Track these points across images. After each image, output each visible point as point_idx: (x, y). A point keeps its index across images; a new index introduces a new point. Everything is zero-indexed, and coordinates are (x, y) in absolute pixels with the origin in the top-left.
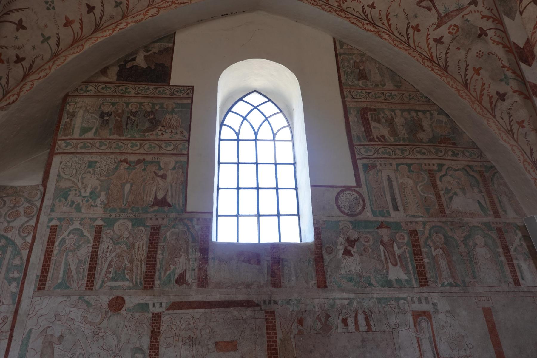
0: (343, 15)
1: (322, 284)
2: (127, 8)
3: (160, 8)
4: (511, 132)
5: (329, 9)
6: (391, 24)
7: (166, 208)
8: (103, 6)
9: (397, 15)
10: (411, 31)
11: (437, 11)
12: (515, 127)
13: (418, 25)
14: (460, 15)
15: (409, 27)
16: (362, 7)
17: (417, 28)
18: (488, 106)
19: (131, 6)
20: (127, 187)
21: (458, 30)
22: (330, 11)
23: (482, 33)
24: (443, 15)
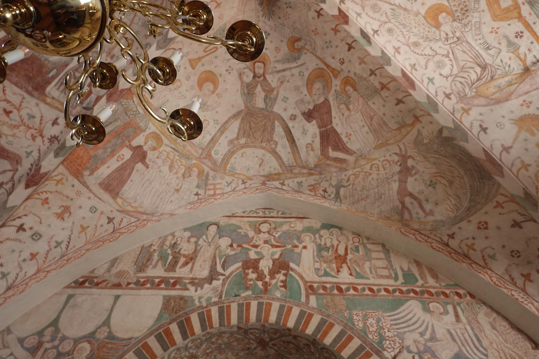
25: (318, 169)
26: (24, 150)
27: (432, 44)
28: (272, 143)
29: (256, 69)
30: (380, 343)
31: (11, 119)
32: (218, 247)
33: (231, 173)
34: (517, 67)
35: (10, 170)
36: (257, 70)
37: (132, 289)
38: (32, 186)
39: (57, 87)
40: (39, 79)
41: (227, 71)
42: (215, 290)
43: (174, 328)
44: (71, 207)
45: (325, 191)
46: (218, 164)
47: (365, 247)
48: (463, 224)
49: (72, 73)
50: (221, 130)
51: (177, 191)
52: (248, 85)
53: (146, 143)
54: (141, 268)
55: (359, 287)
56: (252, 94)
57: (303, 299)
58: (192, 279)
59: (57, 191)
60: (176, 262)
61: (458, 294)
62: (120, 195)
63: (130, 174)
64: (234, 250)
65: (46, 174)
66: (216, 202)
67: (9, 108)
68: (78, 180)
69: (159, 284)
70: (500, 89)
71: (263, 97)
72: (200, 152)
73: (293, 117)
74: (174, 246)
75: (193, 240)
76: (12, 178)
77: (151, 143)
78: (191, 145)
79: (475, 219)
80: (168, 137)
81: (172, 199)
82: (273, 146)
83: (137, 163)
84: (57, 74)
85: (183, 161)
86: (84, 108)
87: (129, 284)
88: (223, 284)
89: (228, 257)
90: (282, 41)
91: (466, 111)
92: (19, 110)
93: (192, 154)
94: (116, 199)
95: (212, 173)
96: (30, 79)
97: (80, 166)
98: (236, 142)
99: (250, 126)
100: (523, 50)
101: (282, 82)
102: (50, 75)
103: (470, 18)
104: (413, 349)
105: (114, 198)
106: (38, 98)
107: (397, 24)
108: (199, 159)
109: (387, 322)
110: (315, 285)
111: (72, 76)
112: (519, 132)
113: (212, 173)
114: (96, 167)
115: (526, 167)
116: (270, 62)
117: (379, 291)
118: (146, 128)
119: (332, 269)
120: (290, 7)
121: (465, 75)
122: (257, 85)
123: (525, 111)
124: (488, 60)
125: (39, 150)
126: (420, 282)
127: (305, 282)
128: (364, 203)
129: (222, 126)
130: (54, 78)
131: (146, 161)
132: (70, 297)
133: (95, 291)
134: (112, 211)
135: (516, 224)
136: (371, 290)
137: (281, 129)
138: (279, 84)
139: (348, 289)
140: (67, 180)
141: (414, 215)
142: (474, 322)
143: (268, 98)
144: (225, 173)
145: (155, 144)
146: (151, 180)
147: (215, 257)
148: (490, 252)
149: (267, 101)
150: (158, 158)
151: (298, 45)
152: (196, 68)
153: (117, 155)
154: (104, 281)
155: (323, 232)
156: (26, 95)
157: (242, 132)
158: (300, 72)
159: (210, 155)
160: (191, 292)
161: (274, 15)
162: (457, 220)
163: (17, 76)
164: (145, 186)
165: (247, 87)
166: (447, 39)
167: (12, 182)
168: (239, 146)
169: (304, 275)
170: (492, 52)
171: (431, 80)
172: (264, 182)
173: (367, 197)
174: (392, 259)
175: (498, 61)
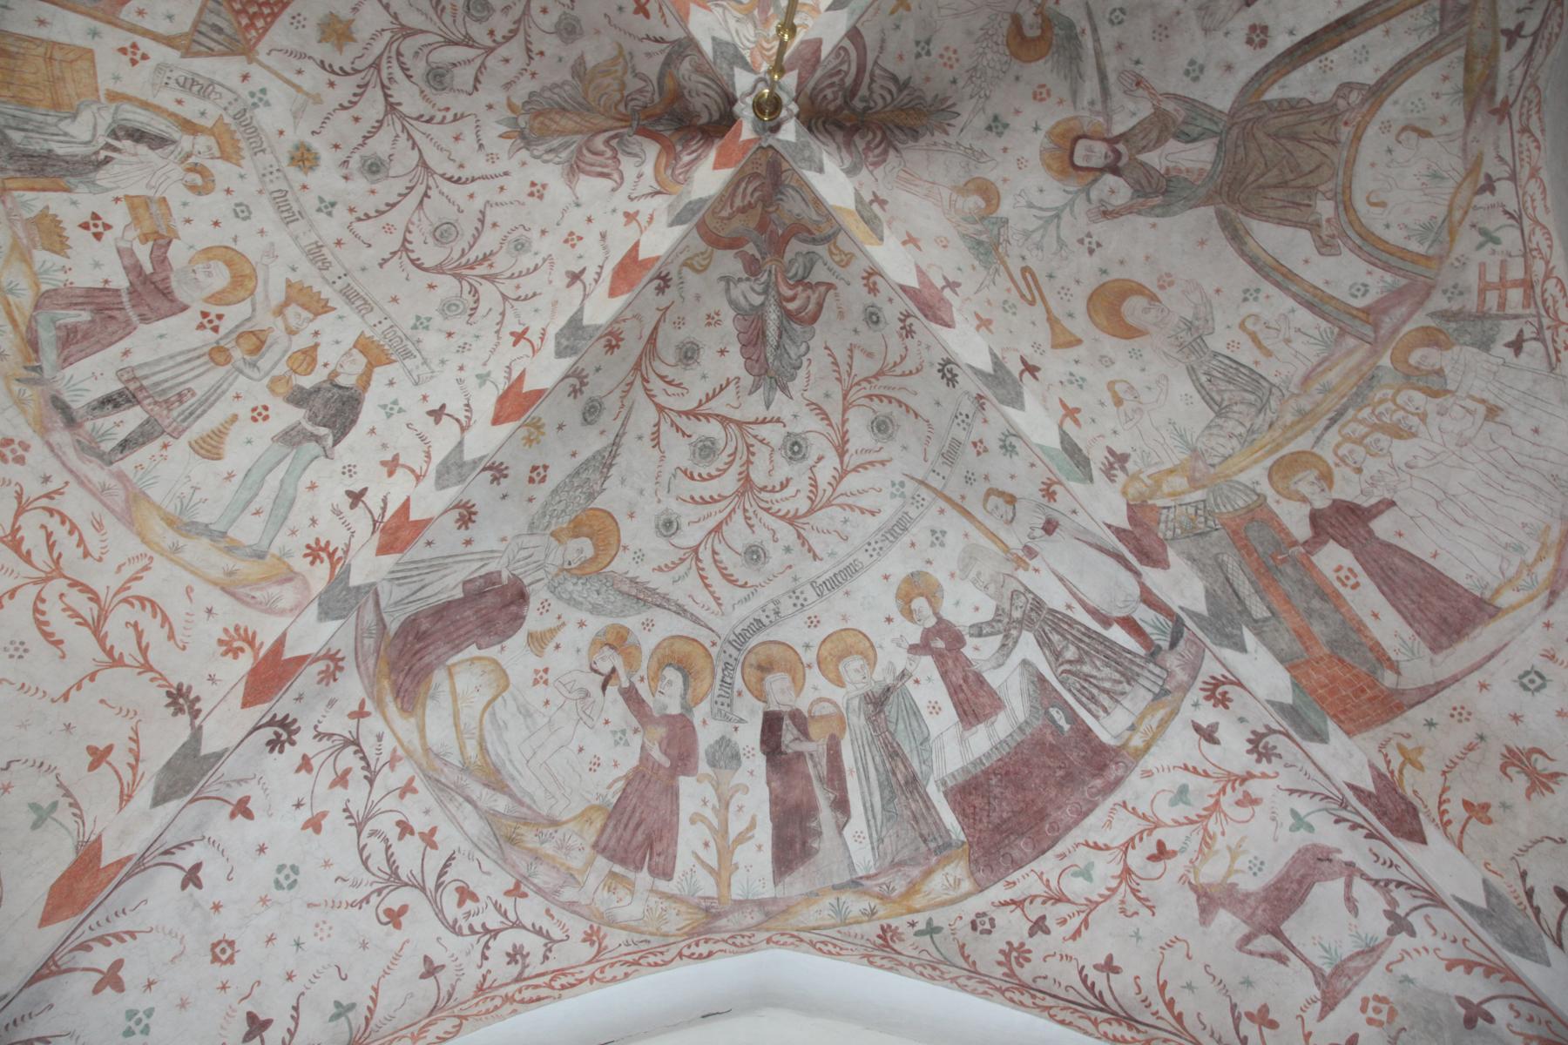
0: (1027, 999)
2: (367, 1020)
3: (466, 1018)
5: (982, 988)
6: (1180, 1014)
8: (296, 1019)
9: (1189, 986)
10: (1248, 1028)
11: (1304, 960)
13: (1264, 1009)
14: (1376, 967)
15: (1239, 1018)
16: (1080, 972)
19: (379, 1014)
21: (1392, 1013)
22: (985, 993)
24: (1328, 970)
26: (1284, 832)
28: (1342, 103)
29: (1092, 164)
31: (1183, 850)
33: (1445, 236)
35: (1349, 885)
36: (1097, 161)
38: (1419, 823)
39: (1101, 713)
40: (1074, 756)
41: (1091, 251)
44: (1512, 746)
46: (1403, 282)
49: (1067, 667)
50: (1280, 278)
51: (1492, 412)
52: (1140, 191)
53: (1304, 500)
56: (1169, 180)
59: (1444, 773)
62: (1487, 595)
63: (1411, 558)
65: (1378, 776)
66: (1560, 272)
68: (1412, 706)
71: (1181, 146)
72: (1351, 342)
73: (1258, 35)
76: (1376, 883)
77: (1305, 483)
78: (1324, 372)
80: (1289, 434)
81: (1524, 429)
82: (1355, 97)
83: (1370, 532)
84: (1065, 707)
85: (1379, 395)
86: (1173, 645)
90: (1017, 78)
92: (1157, 825)
93: (1361, 363)
94: (1498, 609)
95: (1438, 302)
97: (1363, 691)
98: (1326, 231)
99: (1275, 186)
101: (1138, 84)
102: (1066, 727)
106: (1129, 769)
108: (1376, 348)
111: (1073, 668)
113: (1438, 302)
114: (1371, 649)
116: (1075, 118)
118: (1254, 491)
120: (928, 42)
122: (1143, 164)
125: (1292, 792)
129: (1266, 277)
130: (1073, 718)
131: (1366, 505)
134: (1548, 625)
137: (1297, 76)
138: (1146, 94)
140: (1408, 736)
143: (1186, 129)
144: (1441, 259)
145: (1312, 475)
146: (1439, 495)
149: (1195, 131)
150: (1359, 470)
151: (1031, 27)
152: (1079, 335)
153: (1337, 585)
156: (1117, 797)
157: (1292, 213)
158: (1111, 22)
159: (1367, 311)
161: (945, 99)
163: (1059, 808)
164: (1461, 517)
165: (1146, 195)
167: (1392, 886)
168: (1343, 217)
172: (1494, 112)
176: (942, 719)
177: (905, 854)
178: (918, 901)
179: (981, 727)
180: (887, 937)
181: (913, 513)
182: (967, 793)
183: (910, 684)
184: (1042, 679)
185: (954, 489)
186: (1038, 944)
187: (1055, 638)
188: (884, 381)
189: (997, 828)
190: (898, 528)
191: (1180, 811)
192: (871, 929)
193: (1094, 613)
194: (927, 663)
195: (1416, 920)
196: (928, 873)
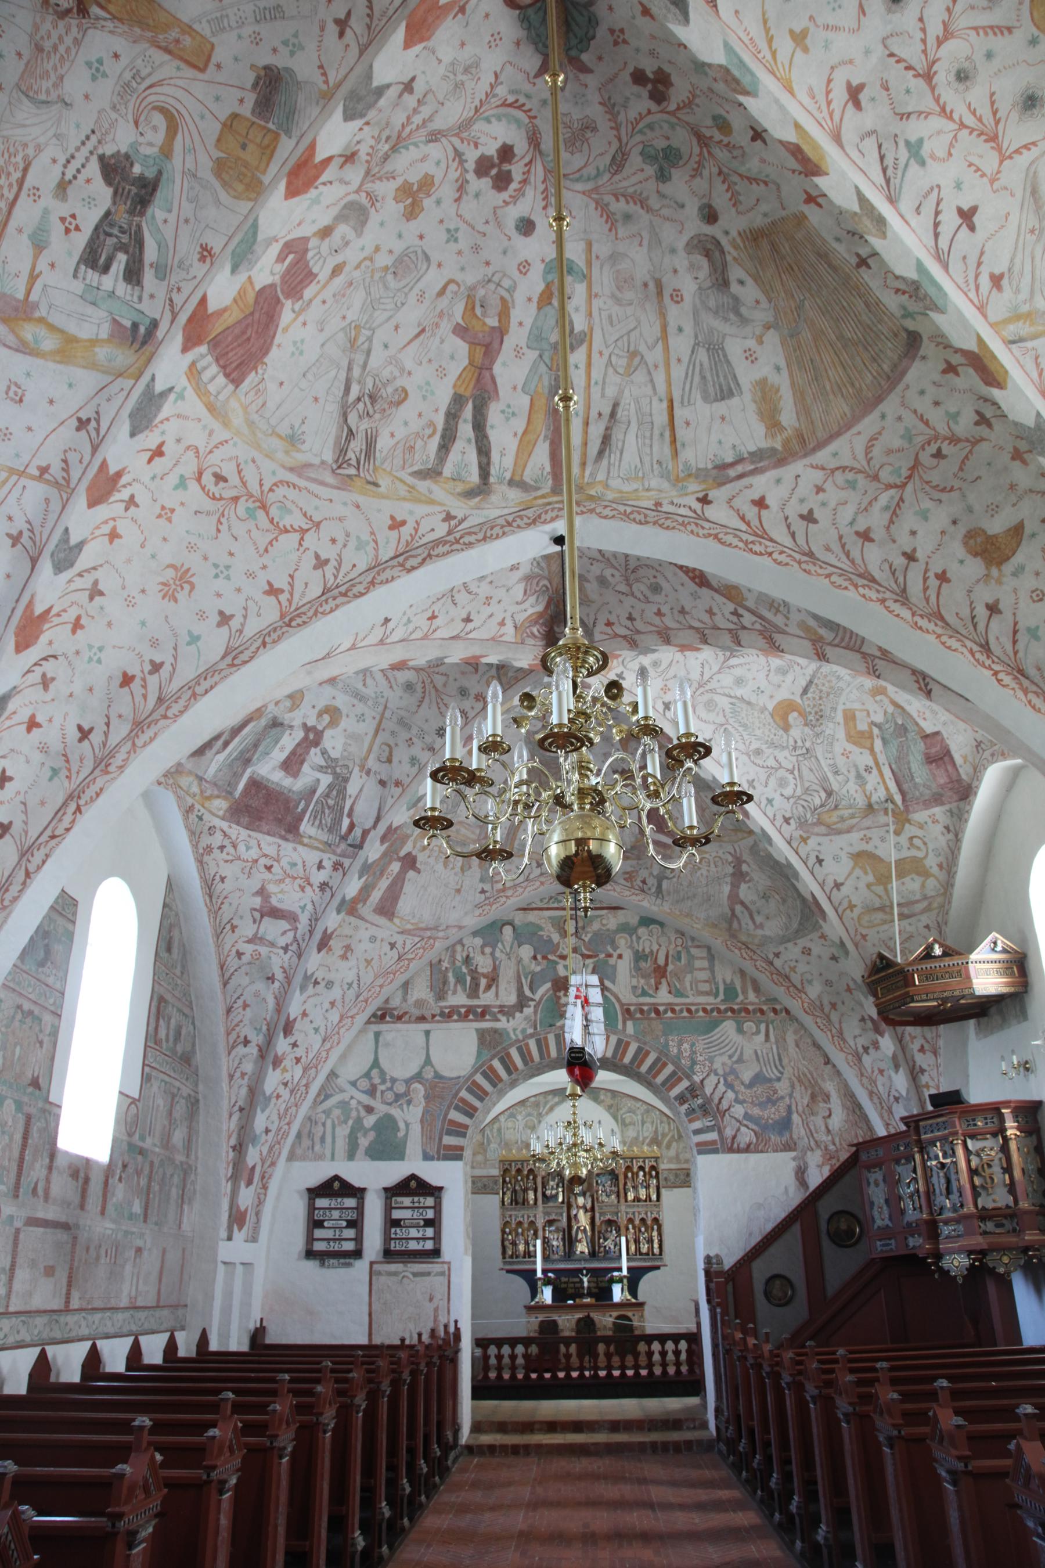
1: (103, 1213)
4: (231, 1077)
7: (37, 1092)
10: (228, 927)
12: (238, 1074)
17: (233, 928)
18: (231, 1042)
20: (18, 1050)
23: (271, 979)
25: (636, 852)
27: (777, 752)
30: (692, 1067)
32: (520, 961)
34: (861, 801)
37: (438, 1022)
40: (289, 818)
42: (526, 1018)
43: (496, 1064)
45: (644, 882)
47: (688, 952)
48: (790, 945)
51: (458, 891)
54: (441, 996)
55: (677, 1008)
57: (620, 1027)
58: (501, 1006)
60: (477, 985)
61: (775, 1011)
64: (539, 964)
66: (509, 902)
67: (269, 863)
69: (466, 1016)
70: (842, 819)
74: (467, 960)
75: (488, 950)
79: (802, 942)
87: (434, 1016)
88: (535, 1012)
89: (534, 974)
91: (804, 840)
92: (278, 861)
96: (279, 821)
100: (869, 787)
103: (823, 727)
104: (720, 1072)
105: (391, 920)
107: (736, 725)
109: (700, 1047)
110: (632, 1008)
112: (853, 868)
115: (851, 907)
117: (697, 1011)
119: (650, 987)
121: (809, 798)
123: (864, 847)
124: (835, 787)
126: (741, 998)
127: (622, 1005)
128: (689, 903)
130: (304, 811)
132: (377, 1035)
133: (399, 1026)
135: (834, 958)
136: (689, 1011)
139: (665, 1012)
141: (744, 926)
142: (781, 1041)
147: (519, 977)
148: (808, 976)
154: (406, 1013)
155: (642, 931)
160: (503, 1023)
162: (784, 940)
166: (795, 748)
169: (621, 996)
170: (840, 778)
171: (770, 801)
173: (694, 896)
174: (716, 968)
175: (844, 790)
176: (279, 755)
177: (220, 783)
178: (207, 804)
179: (283, 773)
180: (191, 808)
181: (370, 703)
182: (256, 785)
183: (288, 732)
184: (314, 792)
185: (389, 725)
186: (216, 851)
187: (335, 793)
188: (433, 691)
189: (247, 806)
190: (362, 698)
191: (287, 867)
192: (190, 801)
193: (351, 810)
194: (299, 734)
195: (290, 953)
196: (218, 797)
